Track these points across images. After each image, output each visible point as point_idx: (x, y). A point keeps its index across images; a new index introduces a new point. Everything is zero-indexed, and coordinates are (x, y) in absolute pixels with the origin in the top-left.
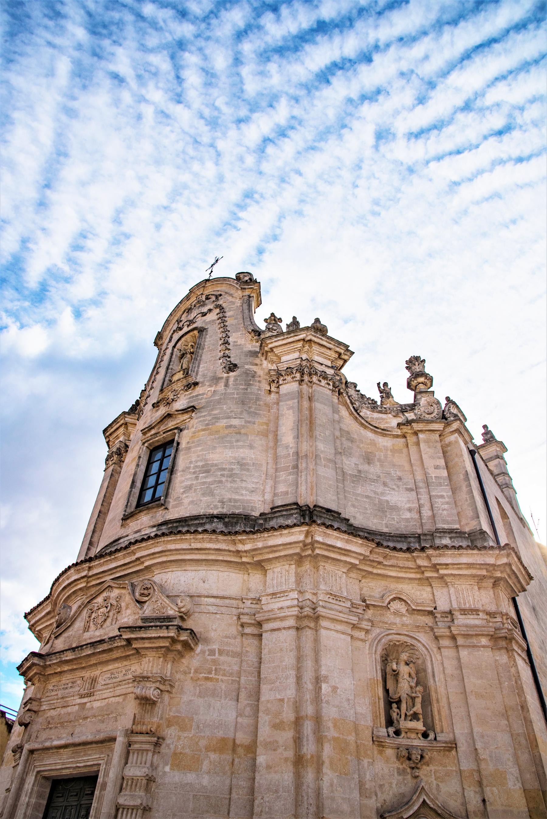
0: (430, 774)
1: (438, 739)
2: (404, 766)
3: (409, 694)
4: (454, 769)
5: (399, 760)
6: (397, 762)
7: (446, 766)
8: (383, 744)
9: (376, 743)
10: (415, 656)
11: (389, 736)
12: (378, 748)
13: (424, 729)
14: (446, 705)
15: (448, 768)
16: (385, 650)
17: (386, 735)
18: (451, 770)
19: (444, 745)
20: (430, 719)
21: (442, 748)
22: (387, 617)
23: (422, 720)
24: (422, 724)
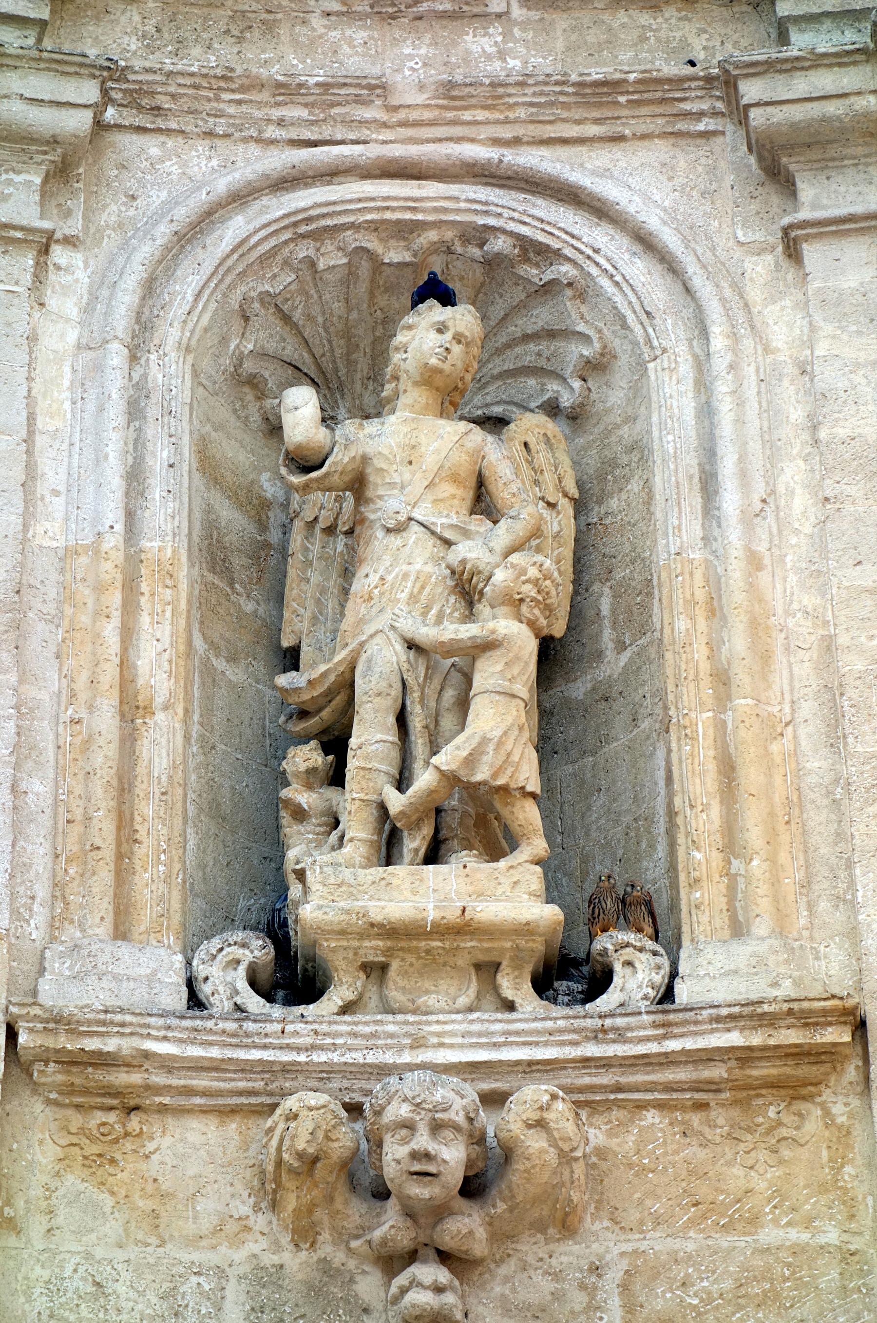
0: (579, 1299)
1: (683, 992)
2: (327, 1248)
3: (426, 633)
4: (832, 1236)
5: (274, 1205)
6: (260, 1221)
7: (754, 1221)
8: (122, 1078)
9: (52, 1075)
10: (577, 351)
11: (195, 1001)
12: (76, 1120)
13: (552, 913)
14: (807, 709)
15: (769, 1235)
16: (265, 318)
17: (178, 999)
18: (797, 1250)
19: (734, 1038)
20: (661, 851)
21: (717, 1072)
22: (307, 48)
23: (539, 845)
24: (534, 877)
